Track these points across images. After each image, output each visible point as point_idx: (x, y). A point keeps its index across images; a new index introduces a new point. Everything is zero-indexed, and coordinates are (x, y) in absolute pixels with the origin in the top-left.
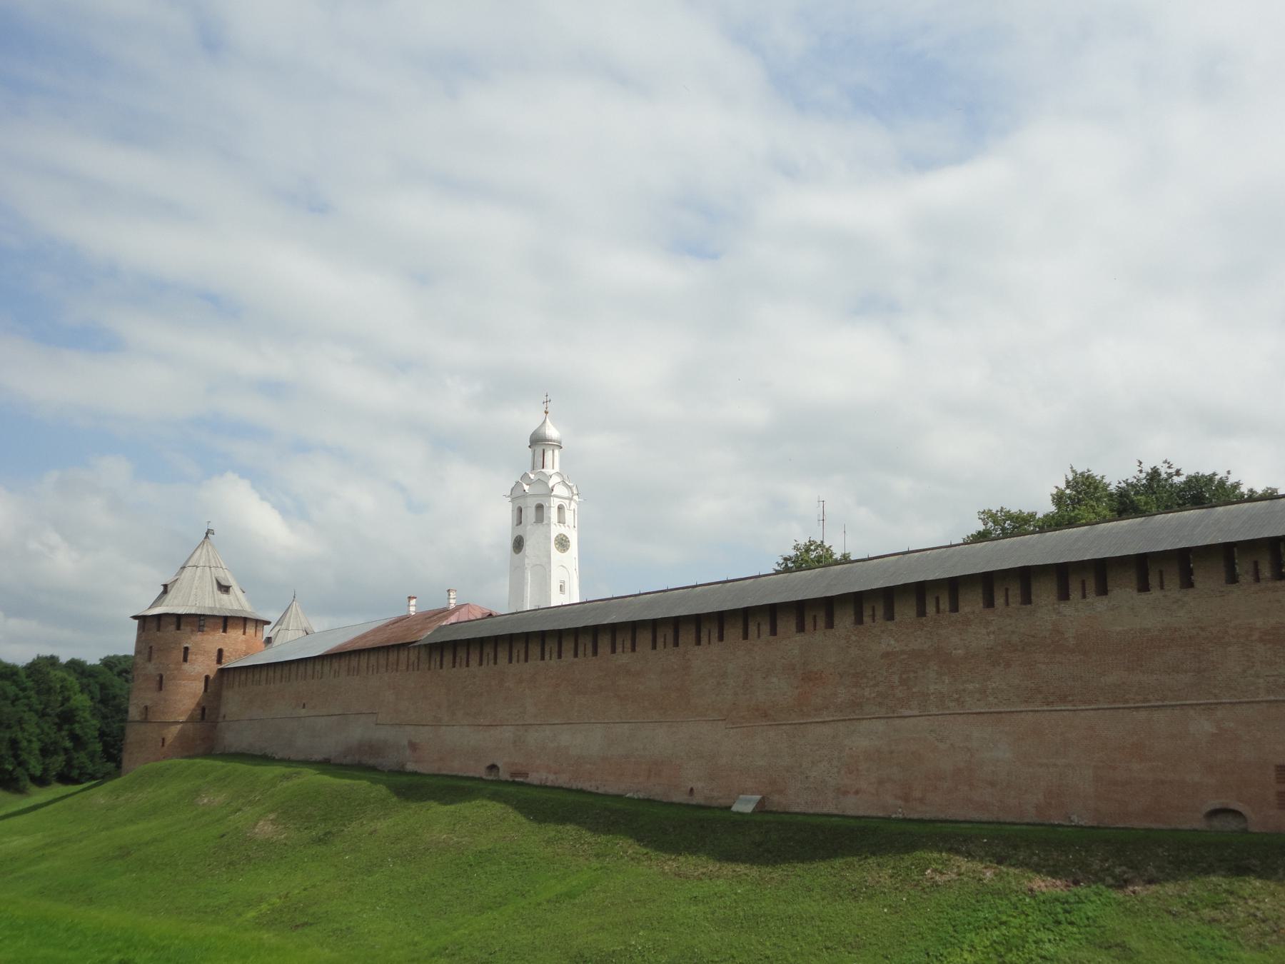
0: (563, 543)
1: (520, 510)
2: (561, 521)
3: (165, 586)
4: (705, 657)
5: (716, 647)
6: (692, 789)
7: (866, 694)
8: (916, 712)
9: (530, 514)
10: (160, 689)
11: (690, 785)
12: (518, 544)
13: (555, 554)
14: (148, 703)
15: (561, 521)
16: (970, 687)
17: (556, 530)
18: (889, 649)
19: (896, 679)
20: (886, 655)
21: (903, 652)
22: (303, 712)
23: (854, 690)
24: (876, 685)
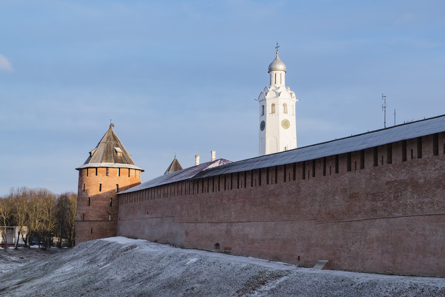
0: (286, 124)
1: (263, 106)
2: (285, 112)
3: (90, 153)
4: (307, 185)
5: (312, 181)
6: (299, 257)
7: (378, 205)
8: (401, 214)
9: (269, 109)
10: (89, 205)
11: (299, 254)
12: (263, 126)
13: (282, 130)
14: (84, 212)
15: (285, 112)
16: (426, 200)
17: (282, 117)
18: (389, 180)
19: (392, 195)
20: (388, 183)
21: (396, 181)
22: (147, 216)
23: (373, 203)
24: (383, 200)
